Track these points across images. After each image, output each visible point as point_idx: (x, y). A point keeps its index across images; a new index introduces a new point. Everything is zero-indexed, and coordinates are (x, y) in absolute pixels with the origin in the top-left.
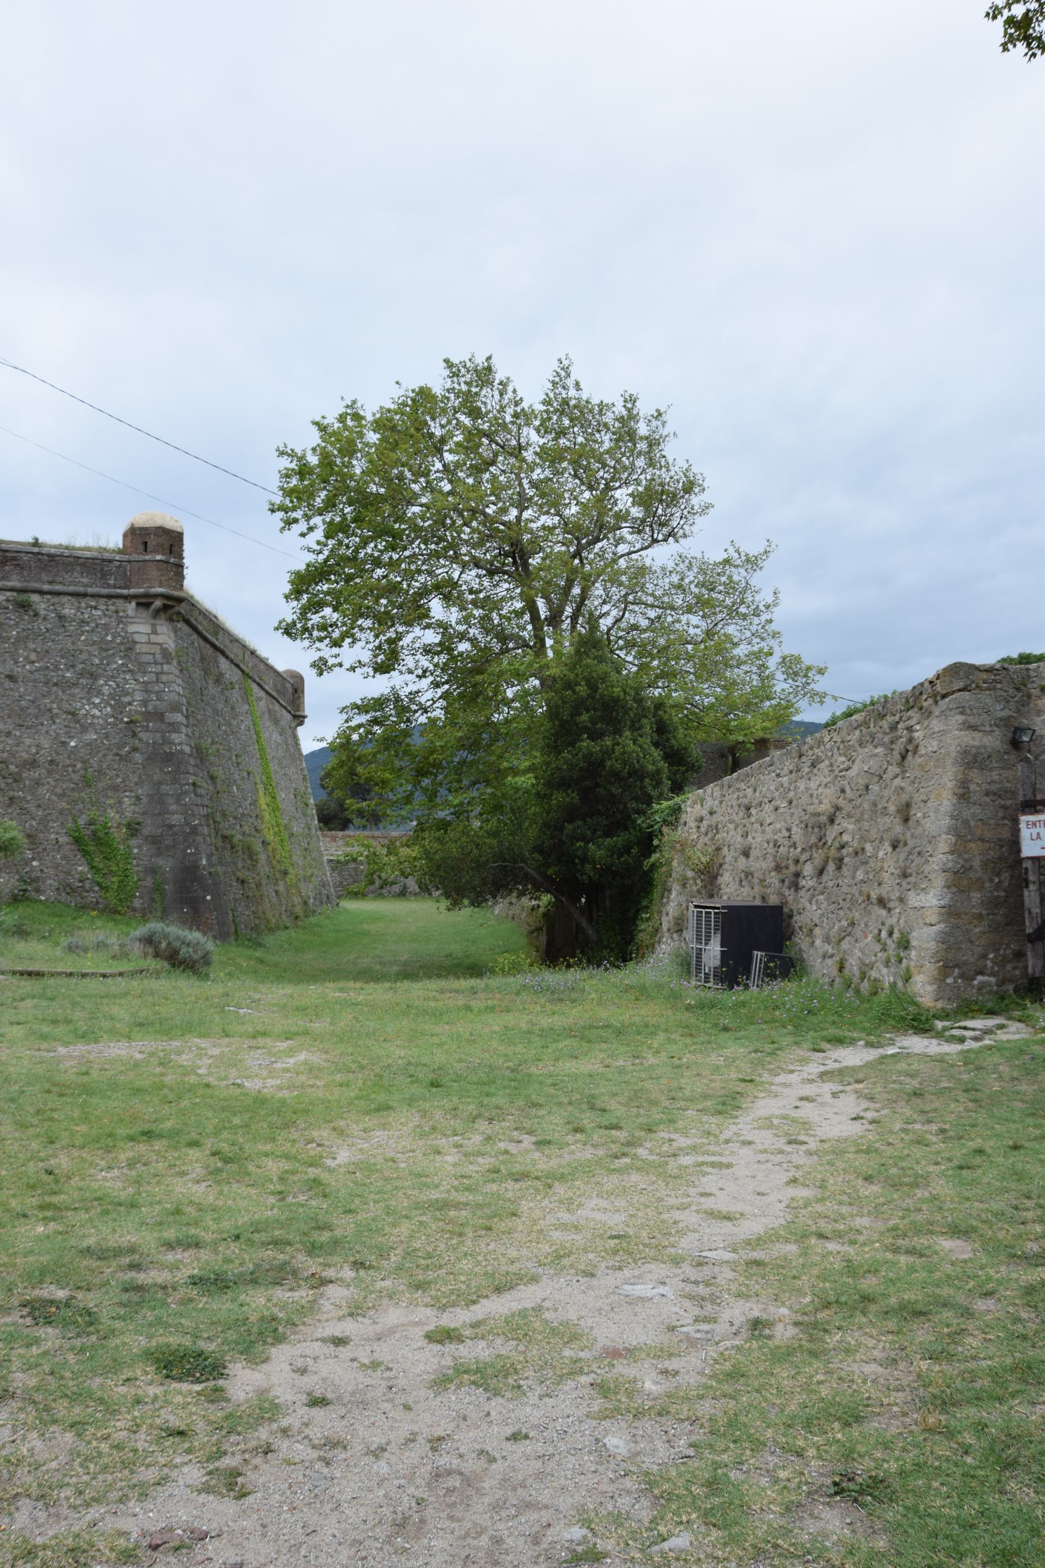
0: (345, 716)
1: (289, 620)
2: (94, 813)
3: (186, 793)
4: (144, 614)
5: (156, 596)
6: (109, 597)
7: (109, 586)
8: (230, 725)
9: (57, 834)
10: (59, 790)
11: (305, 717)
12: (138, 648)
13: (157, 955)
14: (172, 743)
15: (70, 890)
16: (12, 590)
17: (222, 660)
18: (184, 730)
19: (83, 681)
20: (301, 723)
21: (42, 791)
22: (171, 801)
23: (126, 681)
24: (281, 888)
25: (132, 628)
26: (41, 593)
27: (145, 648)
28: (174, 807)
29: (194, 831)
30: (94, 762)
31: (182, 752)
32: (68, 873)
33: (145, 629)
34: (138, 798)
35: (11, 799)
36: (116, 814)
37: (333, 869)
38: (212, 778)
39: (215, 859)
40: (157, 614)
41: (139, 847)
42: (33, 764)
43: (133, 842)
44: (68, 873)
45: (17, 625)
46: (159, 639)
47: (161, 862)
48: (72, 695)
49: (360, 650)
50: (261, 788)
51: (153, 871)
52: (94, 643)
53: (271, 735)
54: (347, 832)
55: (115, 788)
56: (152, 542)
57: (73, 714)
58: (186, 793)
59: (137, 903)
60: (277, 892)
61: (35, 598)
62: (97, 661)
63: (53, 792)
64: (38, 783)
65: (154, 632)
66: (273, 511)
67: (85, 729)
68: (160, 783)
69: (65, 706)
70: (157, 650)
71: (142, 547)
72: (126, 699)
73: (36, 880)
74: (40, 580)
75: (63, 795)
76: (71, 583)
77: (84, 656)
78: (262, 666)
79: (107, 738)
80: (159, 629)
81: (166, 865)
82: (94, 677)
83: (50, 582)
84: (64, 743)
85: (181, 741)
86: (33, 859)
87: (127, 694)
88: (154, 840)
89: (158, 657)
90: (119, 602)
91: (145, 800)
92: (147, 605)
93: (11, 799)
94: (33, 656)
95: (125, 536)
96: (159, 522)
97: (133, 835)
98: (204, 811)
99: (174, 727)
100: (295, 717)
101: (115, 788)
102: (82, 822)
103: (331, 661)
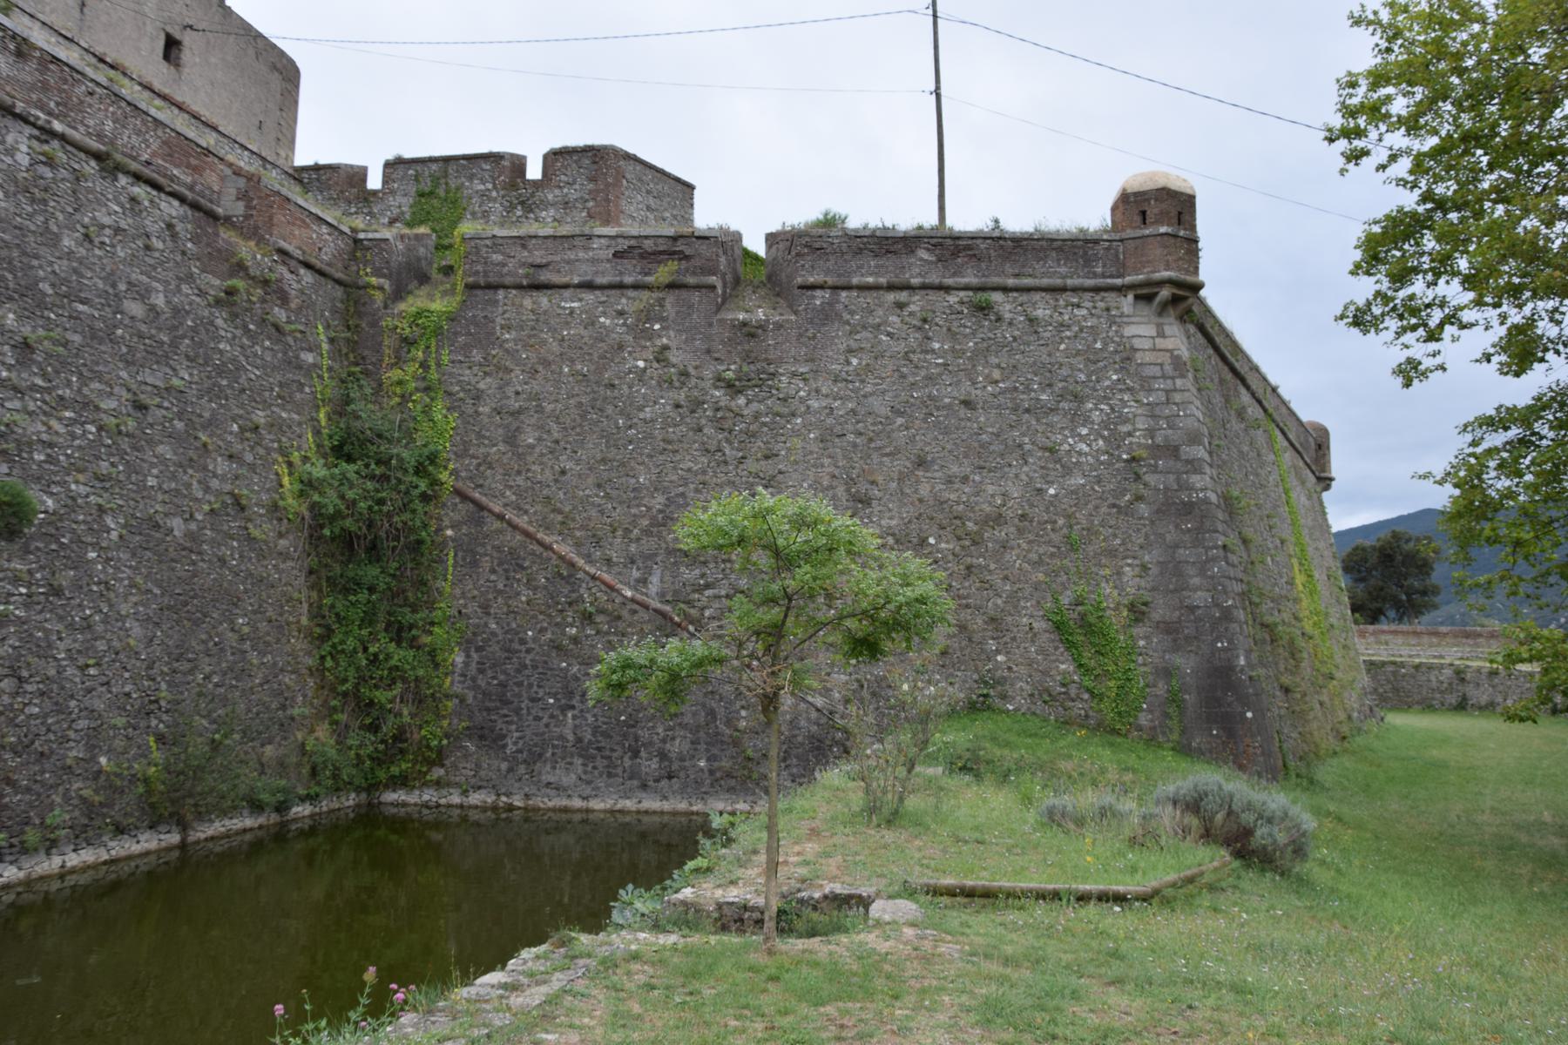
0: (1469, 437)
1: (1361, 302)
2: (1082, 588)
3: (1214, 559)
4: (1146, 310)
6: (1097, 290)
7: (1095, 275)
8: (1257, 475)
9: (1030, 618)
11: (1331, 479)
12: (1139, 357)
13: (1207, 835)
14: (1191, 488)
15: (1049, 698)
16: (966, 288)
17: (1243, 391)
18: (1207, 470)
19: (1065, 405)
20: (1327, 488)
21: (1010, 556)
22: (1191, 571)
23: (1124, 403)
24: (1325, 698)
25: (1128, 331)
27: (1149, 357)
28: (1196, 581)
29: (1227, 615)
30: (1081, 516)
31: (1206, 501)
32: (1045, 673)
34: (1144, 568)
35: (968, 568)
37: (1368, 671)
38: (1245, 541)
39: (1254, 656)
42: (998, 519)
43: (1138, 631)
44: (1045, 673)
45: (974, 334)
47: (1178, 660)
49: (1486, 330)
50: (1295, 561)
51: (1167, 673)
52: (1078, 353)
53: (1299, 498)
54: (1377, 627)
55: (1112, 553)
56: (1153, 210)
57: (1051, 450)
58: (1214, 559)
59: (1144, 719)
60: (1321, 704)
61: (997, 297)
62: (1083, 377)
63: (1025, 559)
65: (1161, 334)
66: (1331, 140)
67: (1068, 471)
68: (1177, 546)
69: (1041, 440)
70: (1166, 358)
71: (1138, 219)
73: (1001, 682)
75: (1039, 563)
76: (1044, 275)
77: (1064, 372)
78: (1284, 410)
80: (1168, 330)
81: (1186, 663)
82: (1078, 398)
83: (1017, 276)
85: (1203, 485)
86: (998, 652)
87: (1126, 421)
89: (1168, 369)
90: (1111, 297)
91: (1154, 570)
92: (1149, 298)
93: (968, 568)
94: (996, 374)
95: (1114, 209)
96: (1161, 183)
97: (1137, 620)
98: (1238, 588)
99: (1194, 466)
100: (1319, 479)
101: (1112, 553)
102: (1065, 600)
103: (1428, 363)
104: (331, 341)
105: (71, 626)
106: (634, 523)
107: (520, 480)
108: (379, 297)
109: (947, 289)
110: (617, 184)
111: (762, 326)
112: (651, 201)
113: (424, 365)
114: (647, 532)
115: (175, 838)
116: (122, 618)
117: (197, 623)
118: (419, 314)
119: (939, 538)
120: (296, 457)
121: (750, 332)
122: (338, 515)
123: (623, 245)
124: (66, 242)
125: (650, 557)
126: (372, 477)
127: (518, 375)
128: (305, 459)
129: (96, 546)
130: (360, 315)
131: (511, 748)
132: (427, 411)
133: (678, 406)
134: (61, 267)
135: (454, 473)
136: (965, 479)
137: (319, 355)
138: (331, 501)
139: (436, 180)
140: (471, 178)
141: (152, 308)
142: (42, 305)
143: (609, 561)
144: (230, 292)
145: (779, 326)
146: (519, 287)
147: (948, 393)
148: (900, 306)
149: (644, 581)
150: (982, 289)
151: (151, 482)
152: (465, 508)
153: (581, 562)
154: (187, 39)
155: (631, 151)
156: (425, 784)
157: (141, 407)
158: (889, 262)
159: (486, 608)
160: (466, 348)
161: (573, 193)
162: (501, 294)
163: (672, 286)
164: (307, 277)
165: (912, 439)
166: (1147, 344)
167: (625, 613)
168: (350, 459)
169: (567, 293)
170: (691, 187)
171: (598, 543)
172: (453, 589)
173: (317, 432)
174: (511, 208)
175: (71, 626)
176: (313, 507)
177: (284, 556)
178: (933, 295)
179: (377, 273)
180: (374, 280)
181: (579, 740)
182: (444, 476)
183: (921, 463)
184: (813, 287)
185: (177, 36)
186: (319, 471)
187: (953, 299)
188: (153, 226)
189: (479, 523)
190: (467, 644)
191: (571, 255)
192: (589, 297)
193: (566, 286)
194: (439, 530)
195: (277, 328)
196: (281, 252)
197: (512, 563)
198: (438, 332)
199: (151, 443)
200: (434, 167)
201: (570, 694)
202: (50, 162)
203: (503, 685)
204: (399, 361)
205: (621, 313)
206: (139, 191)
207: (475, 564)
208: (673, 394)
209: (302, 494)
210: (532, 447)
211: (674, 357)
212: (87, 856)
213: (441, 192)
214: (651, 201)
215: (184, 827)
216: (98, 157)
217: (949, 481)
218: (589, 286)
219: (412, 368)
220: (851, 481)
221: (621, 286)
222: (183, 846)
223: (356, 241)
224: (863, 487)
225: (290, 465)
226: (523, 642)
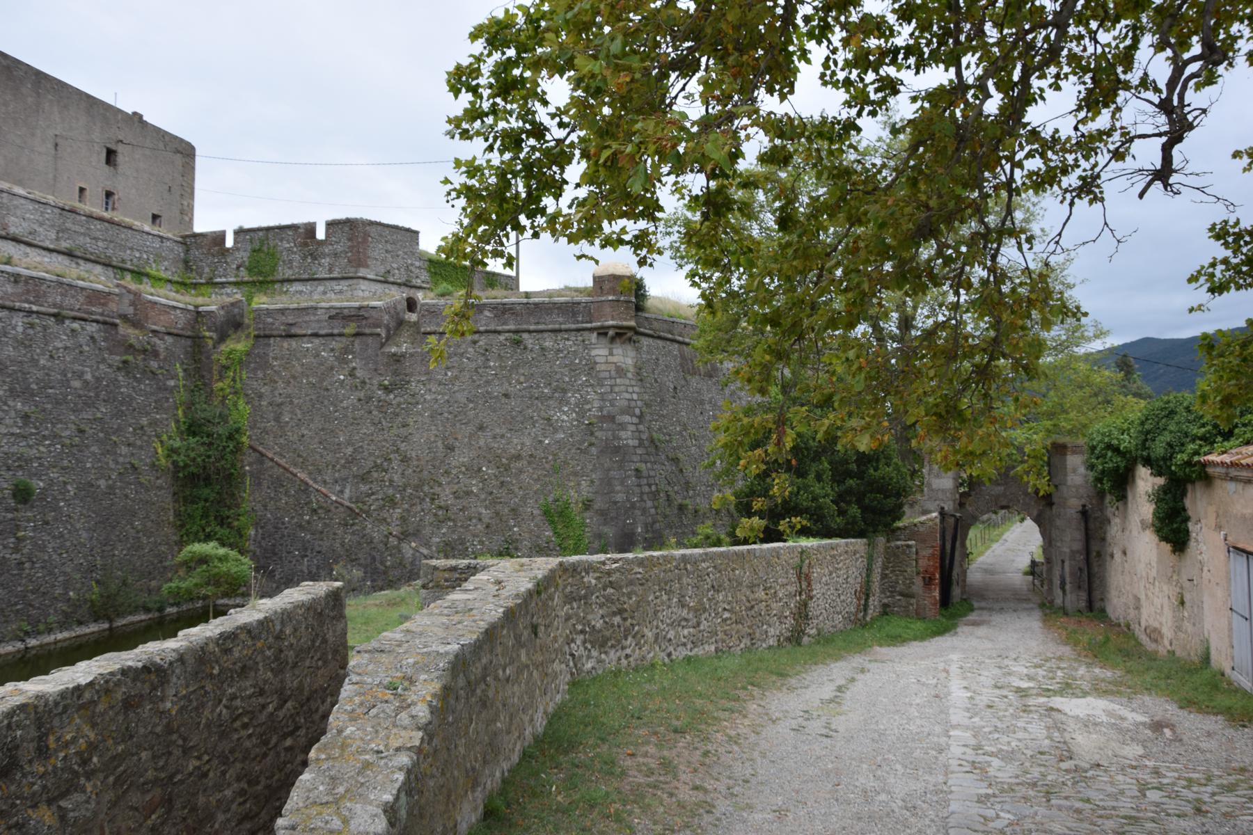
3: (629, 476)
4: (604, 341)
6: (578, 330)
7: (578, 322)
9: (532, 508)
10: (535, 476)
12: (598, 367)
14: (620, 439)
19: (556, 395)
25: (594, 353)
26: (529, 332)
27: (603, 367)
28: (618, 488)
30: (561, 455)
31: (627, 445)
33: (605, 352)
34: (592, 482)
35: (502, 483)
36: (577, 492)
40: (613, 340)
41: (591, 518)
42: (518, 457)
43: (587, 514)
46: (614, 359)
47: (606, 529)
48: (548, 406)
52: (566, 366)
55: (575, 474)
58: (629, 476)
61: (525, 336)
64: (521, 471)
65: (611, 354)
67: (556, 431)
70: (613, 367)
72: (587, 407)
74: (529, 323)
75: (538, 479)
76: (551, 323)
77: (558, 376)
79: (572, 436)
80: (615, 351)
82: (564, 391)
84: (541, 442)
87: (588, 402)
88: (602, 513)
89: (613, 373)
90: (586, 334)
91: (597, 483)
93: (502, 483)
94: (522, 379)
99: (622, 426)
101: (575, 474)
102: (550, 499)
104: (185, 370)
105: (54, 537)
106: (337, 462)
107: (282, 441)
108: (210, 343)
109: (499, 332)
110: (365, 241)
111: (403, 355)
112: (389, 247)
113: (234, 380)
114: (344, 467)
115: (106, 626)
116: (77, 531)
117: (114, 527)
118: (230, 353)
119: (488, 468)
120: (165, 437)
121: (397, 358)
122: (186, 466)
123: (333, 312)
124: (42, 362)
125: (345, 479)
126: (203, 444)
127: (281, 384)
128: (170, 438)
129: (63, 500)
130: (200, 352)
131: (278, 577)
132: (235, 404)
133: (360, 400)
134: (40, 374)
135: (249, 437)
136: (502, 436)
137: (178, 378)
138: (181, 459)
139: (262, 242)
140: (281, 240)
141: (86, 382)
142: (33, 395)
143: (325, 482)
144: (125, 362)
145: (412, 355)
146: (281, 336)
147: (496, 390)
148: (475, 342)
149: (342, 492)
150: (516, 332)
151: (88, 465)
153: (311, 482)
154: (120, 148)
155: (373, 219)
156: (237, 595)
157: (81, 431)
159: (265, 506)
160: (255, 369)
161: (339, 248)
162: (272, 340)
163: (357, 335)
164: (169, 339)
165: (477, 415)
166: (603, 360)
167: (332, 508)
168: (194, 434)
169: (305, 339)
170: (417, 233)
171: (320, 471)
172: (250, 498)
173: (177, 421)
174: (304, 258)
175: (54, 537)
176: (175, 463)
177: (160, 488)
178: (491, 336)
179: (209, 330)
180: (207, 334)
181: (310, 572)
182: (244, 439)
183: (481, 428)
184: (430, 333)
185: (113, 147)
186: (177, 443)
187: (502, 338)
188: (83, 339)
189: (262, 463)
190: (256, 525)
191: (307, 318)
192: (317, 341)
193: (304, 336)
194: (243, 467)
195: (153, 372)
196: (154, 331)
197: (278, 483)
198: (240, 362)
199: (87, 447)
200: (261, 234)
201: (306, 550)
202: (32, 326)
203: (274, 545)
204: (221, 378)
205: (332, 350)
206: (76, 325)
207: (259, 484)
208: (357, 393)
209: (169, 456)
210: (287, 423)
211: (359, 373)
212: (66, 634)
213: (265, 248)
214: (389, 247)
215: (111, 621)
216: (54, 315)
217: (495, 437)
218: (316, 335)
219: (228, 381)
220: (445, 439)
221: (332, 335)
222: (110, 629)
223: (198, 313)
224: (451, 441)
225: (162, 440)
226: (283, 523)
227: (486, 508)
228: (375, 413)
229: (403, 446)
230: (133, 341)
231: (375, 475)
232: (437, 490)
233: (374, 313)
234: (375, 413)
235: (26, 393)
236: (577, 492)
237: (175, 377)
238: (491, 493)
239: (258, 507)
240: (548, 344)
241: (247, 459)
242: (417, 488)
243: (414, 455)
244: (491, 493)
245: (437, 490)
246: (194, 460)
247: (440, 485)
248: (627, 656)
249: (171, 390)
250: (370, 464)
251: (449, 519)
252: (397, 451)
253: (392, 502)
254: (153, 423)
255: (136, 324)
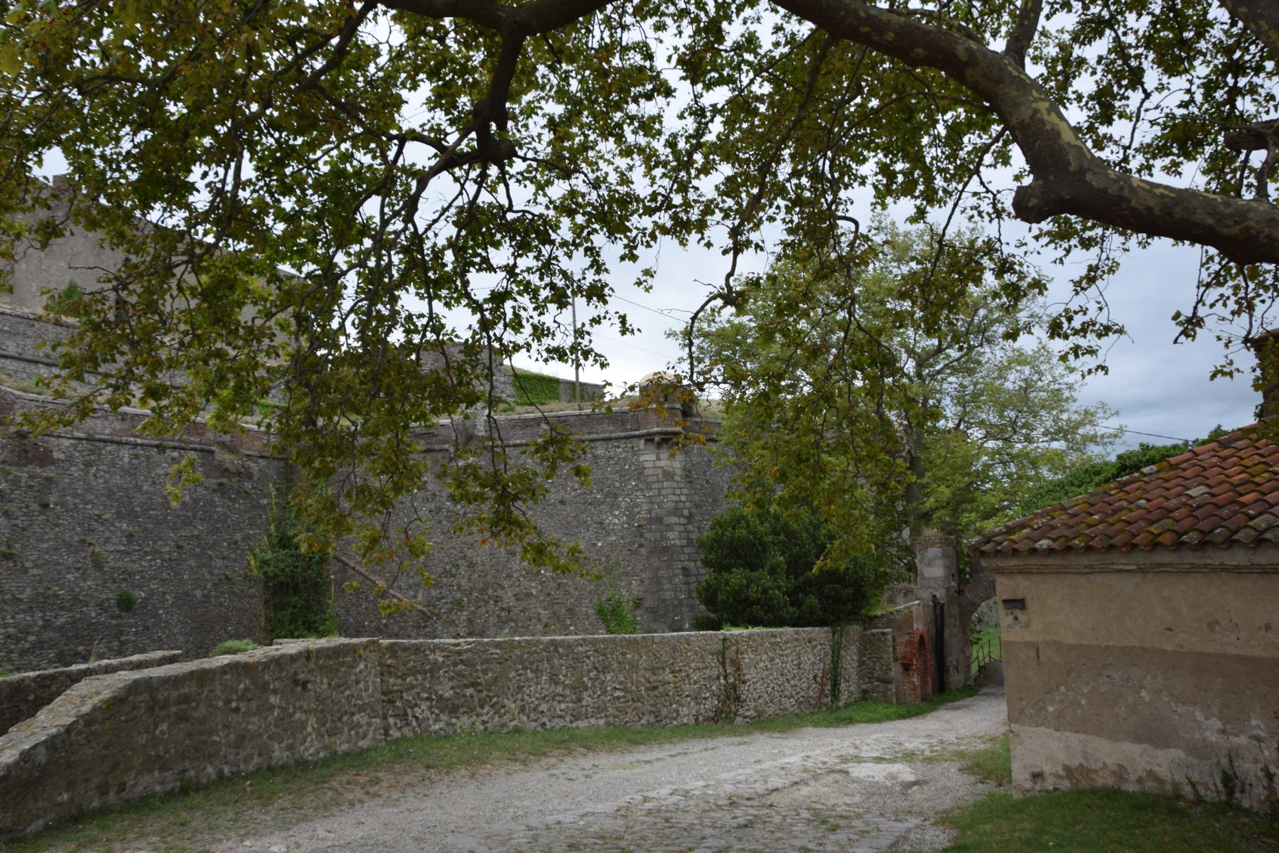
3: (676, 575)
4: (652, 447)
5: (655, 434)
6: (627, 438)
14: (667, 539)
25: (642, 458)
27: (651, 472)
28: (667, 586)
31: (674, 545)
33: (653, 457)
34: (642, 581)
40: (659, 445)
43: (638, 612)
48: (601, 511)
55: (627, 574)
65: (658, 459)
67: (608, 534)
69: (595, 518)
70: (660, 471)
72: (637, 510)
79: (622, 538)
80: (662, 456)
82: (616, 496)
84: (594, 545)
88: (652, 611)
89: (660, 477)
90: (635, 441)
91: (647, 582)
94: (576, 486)
99: (670, 527)
101: (627, 574)
104: (277, 489)
105: (153, 641)
117: (209, 632)
120: (257, 551)
122: (276, 576)
124: (145, 487)
125: (418, 585)
126: (292, 556)
128: (262, 551)
129: (162, 608)
134: (143, 498)
138: (270, 570)
142: (137, 517)
143: (400, 588)
144: (220, 484)
149: (415, 596)
151: (186, 577)
152: (339, 565)
157: (180, 547)
158: (528, 431)
159: (348, 612)
164: (263, 462)
166: (651, 465)
168: (284, 547)
173: (270, 536)
175: (153, 641)
176: (265, 573)
182: (330, 550)
186: (269, 556)
189: (345, 572)
196: (248, 456)
199: (184, 560)
202: (137, 457)
206: (176, 454)
209: (261, 567)
216: (157, 446)
225: (258, 554)
227: (545, 609)
228: (444, 522)
229: (469, 553)
230: (227, 465)
231: (445, 580)
232: (500, 592)
233: (442, 431)
234: (444, 522)
235: (131, 515)
236: (628, 591)
237: (268, 496)
238: (549, 595)
239: (342, 612)
240: (600, 452)
241: (332, 569)
242: (483, 591)
243: (479, 560)
244: (549, 595)
245: (500, 592)
246: (283, 570)
247: (503, 588)
248: (484, 722)
249: (264, 508)
250: (440, 570)
251: (512, 620)
252: (464, 557)
253: (459, 605)
254: (247, 538)
255: (232, 450)
